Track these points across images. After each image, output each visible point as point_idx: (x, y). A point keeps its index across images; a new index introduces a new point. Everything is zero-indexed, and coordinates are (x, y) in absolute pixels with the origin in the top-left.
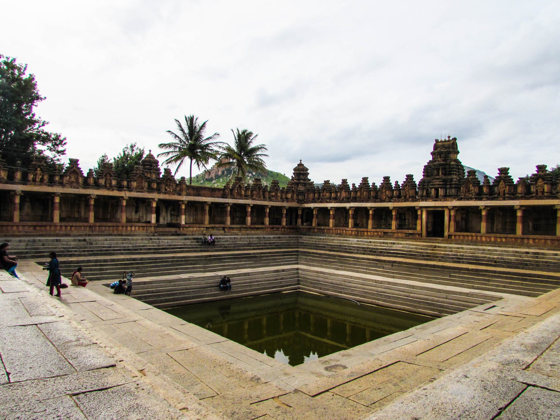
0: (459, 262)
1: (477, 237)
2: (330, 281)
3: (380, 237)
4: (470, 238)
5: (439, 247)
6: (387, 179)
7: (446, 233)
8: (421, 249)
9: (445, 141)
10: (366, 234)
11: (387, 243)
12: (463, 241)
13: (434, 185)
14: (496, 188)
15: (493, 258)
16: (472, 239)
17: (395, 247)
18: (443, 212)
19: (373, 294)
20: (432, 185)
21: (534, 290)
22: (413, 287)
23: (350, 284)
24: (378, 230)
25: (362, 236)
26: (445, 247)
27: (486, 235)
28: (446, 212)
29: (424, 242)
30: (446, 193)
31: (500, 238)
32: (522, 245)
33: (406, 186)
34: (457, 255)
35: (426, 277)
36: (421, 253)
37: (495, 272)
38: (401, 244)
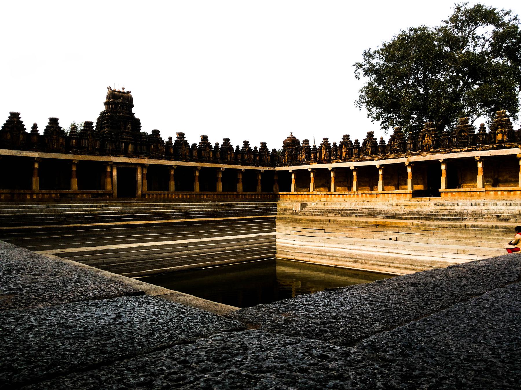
0: (191, 218)
1: (168, 194)
2: (131, 258)
3: (57, 200)
4: (162, 196)
5: (158, 206)
6: (54, 122)
7: (140, 192)
8: (145, 209)
9: (119, 92)
10: (28, 197)
11: (96, 206)
12: (156, 199)
13: (124, 139)
14: (180, 150)
15: (209, 211)
16: (164, 197)
17: (113, 210)
18: (136, 169)
19: (197, 257)
20: (121, 138)
21: (266, 228)
22: (217, 242)
23: (161, 255)
24: (52, 191)
25: (24, 200)
26: (164, 206)
27: (176, 193)
28: (139, 171)
29: (120, 203)
30: (135, 148)
31: (186, 195)
32: (200, 200)
33: (89, 135)
34: (182, 212)
35: (199, 233)
36: (148, 213)
37: (235, 220)
38: (116, 206)
